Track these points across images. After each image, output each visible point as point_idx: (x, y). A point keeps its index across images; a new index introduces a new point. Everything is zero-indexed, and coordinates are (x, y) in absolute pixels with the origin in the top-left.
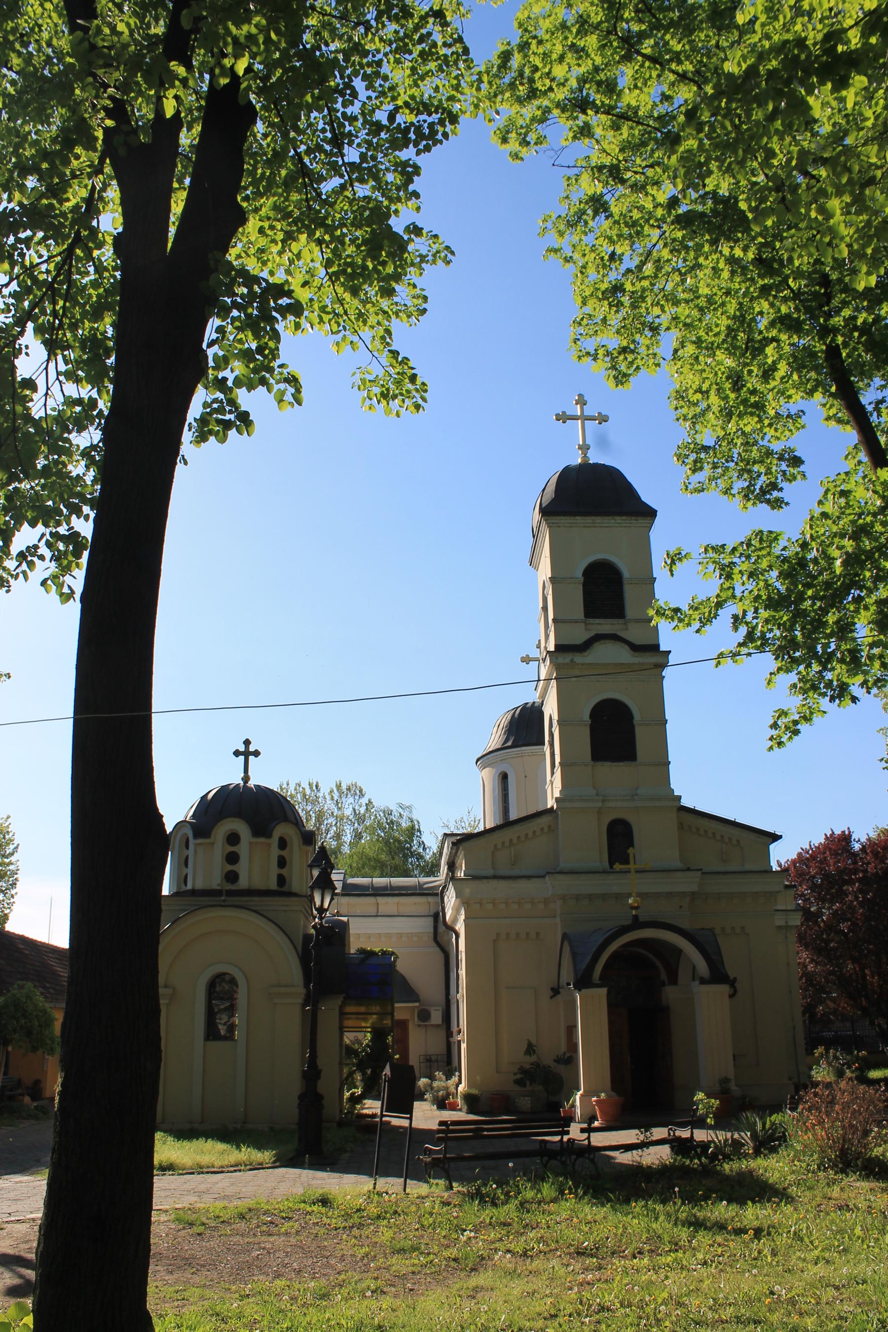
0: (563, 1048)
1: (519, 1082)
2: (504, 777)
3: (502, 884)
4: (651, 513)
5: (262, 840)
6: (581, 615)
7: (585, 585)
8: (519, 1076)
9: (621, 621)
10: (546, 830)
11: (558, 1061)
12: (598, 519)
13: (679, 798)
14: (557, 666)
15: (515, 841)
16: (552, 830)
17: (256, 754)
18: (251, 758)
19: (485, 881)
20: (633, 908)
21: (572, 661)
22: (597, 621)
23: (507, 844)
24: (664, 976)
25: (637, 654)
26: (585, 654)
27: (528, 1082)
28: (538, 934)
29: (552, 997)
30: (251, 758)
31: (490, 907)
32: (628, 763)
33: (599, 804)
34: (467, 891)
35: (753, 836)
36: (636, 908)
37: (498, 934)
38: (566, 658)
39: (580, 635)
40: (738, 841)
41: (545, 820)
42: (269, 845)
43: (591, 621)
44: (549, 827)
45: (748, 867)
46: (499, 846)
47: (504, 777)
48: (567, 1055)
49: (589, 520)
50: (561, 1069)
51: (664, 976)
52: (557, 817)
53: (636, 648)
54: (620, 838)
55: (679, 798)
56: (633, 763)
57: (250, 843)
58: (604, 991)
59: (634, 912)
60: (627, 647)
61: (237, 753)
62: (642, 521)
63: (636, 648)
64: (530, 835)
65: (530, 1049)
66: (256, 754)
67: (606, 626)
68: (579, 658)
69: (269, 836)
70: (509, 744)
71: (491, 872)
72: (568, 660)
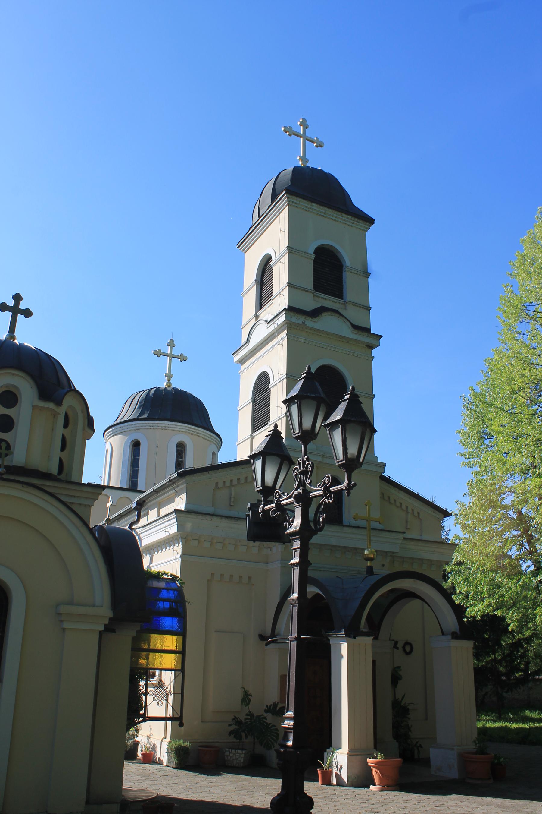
1: (236, 734)
2: (136, 445)
3: (225, 524)
4: (370, 221)
5: (51, 405)
6: (311, 286)
7: (315, 262)
8: (234, 727)
9: (341, 301)
12: (330, 211)
13: (384, 465)
14: (289, 325)
15: (235, 482)
17: (27, 313)
18: (20, 317)
19: (208, 517)
20: (368, 559)
21: (304, 323)
22: (323, 295)
23: (228, 484)
25: (356, 331)
26: (316, 320)
27: (243, 734)
28: (250, 578)
30: (20, 317)
31: (207, 545)
34: (189, 526)
35: (430, 510)
36: (371, 560)
37: (213, 574)
38: (299, 319)
39: (310, 302)
40: (418, 513)
42: (55, 415)
43: (318, 294)
45: (425, 537)
46: (220, 485)
47: (136, 445)
48: (280, 706)
49: (322, 209)
53: (356, 327)
55: (384, 465)
57: (33, 407)
59: (369, 564)
60: (348, 323)
61: (17, 298)
62: (362, 224)
63: (356, 327)
65: (246, 698)
66: (27, 313)
67: (329, 301)
68: (310, 322)
69: (59, 403)
70: (145, 416)
71: (211, 510)
72: (300, 321)
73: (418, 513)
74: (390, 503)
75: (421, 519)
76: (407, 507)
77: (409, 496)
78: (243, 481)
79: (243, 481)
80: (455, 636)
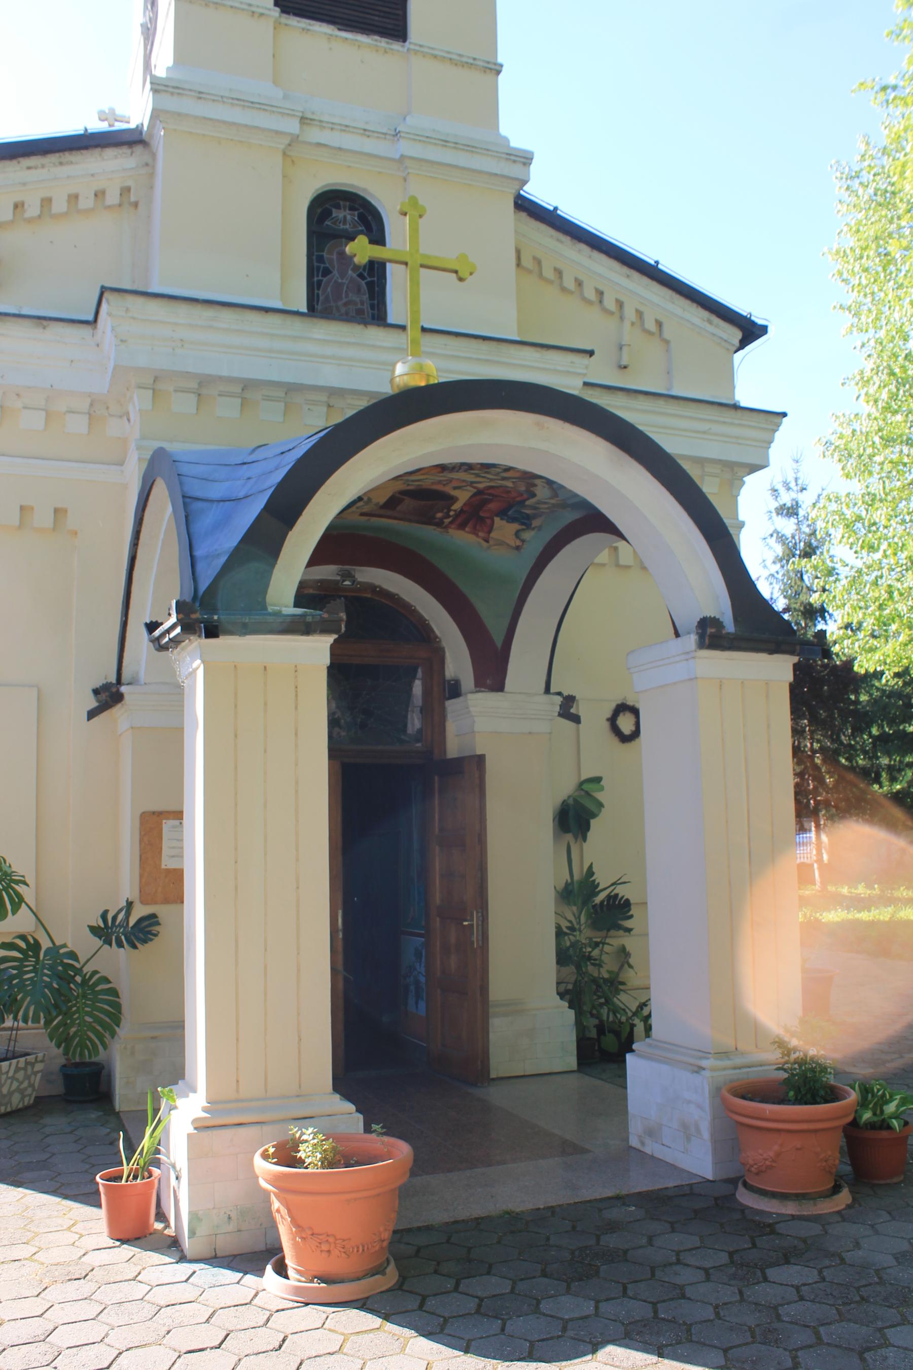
0: (126, 887)
10: (113, 198)
11: (106, 931)
13: (525, 159)
16: (129, 201)
24: (458, 661)
29: (92, 714)
32: (384, 43)
33: (292, 126)
35: (697, 315)
40: (659, 324)
41: (110, 166)
44: (125, 191)
48: (139, 912)
50: (116, 963)
51: (458, 661)
52: (150, 165)
54: (343, 255)
55: (525, 159)
56: (396, 46)
58: (316, 650)
64: (60, 205)
73: (659, 324)
74: (564, 289)
75: (667, 342)
76: (620, 304)
77: (625, 270)
78: (33, 210)
79: (33, 210)
80: (711, 636)
